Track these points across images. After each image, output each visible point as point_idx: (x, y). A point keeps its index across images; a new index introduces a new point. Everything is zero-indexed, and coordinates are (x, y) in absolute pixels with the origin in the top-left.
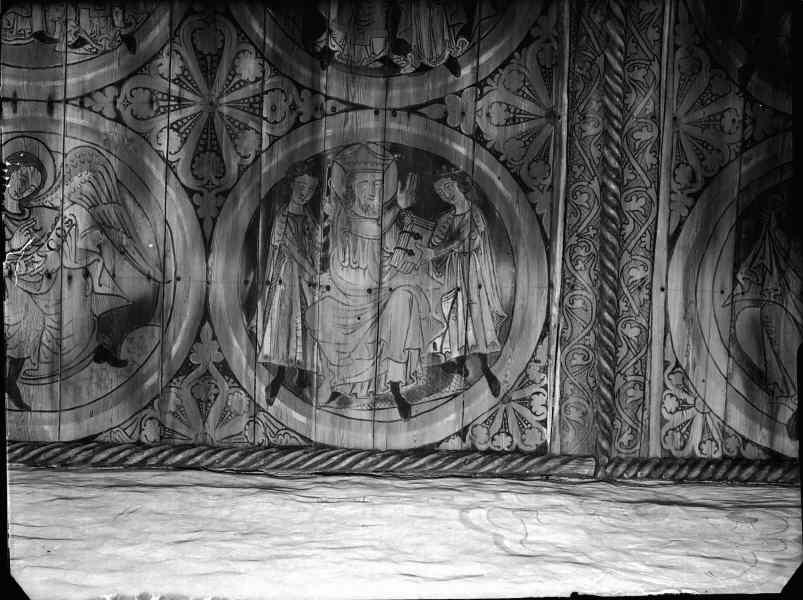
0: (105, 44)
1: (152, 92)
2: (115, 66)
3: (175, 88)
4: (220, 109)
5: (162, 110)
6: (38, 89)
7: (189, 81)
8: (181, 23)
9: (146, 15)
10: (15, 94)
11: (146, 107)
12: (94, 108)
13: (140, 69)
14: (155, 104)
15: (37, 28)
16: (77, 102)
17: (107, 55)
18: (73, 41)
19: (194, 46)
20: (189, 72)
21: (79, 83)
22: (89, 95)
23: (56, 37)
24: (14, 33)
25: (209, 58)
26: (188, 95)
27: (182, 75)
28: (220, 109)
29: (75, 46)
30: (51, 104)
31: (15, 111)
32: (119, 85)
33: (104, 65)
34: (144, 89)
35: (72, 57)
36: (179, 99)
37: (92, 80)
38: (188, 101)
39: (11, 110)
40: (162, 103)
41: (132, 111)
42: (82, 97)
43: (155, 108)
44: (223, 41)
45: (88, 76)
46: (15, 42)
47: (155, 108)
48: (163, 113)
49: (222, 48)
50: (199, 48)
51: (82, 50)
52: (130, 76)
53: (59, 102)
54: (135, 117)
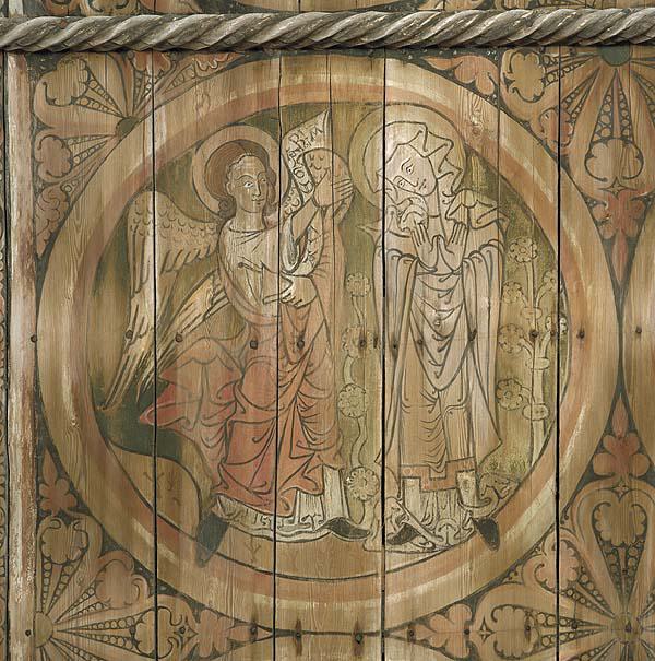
0: (448, 534)
1: (528, 613)
2: (465, 568)
3: (565, 603)
4: (644, 636)
5: (546, 642)
6: (340, 612)
7: (599, 602)
8: (576, 493)
9: (514, 485)
10: (299, 624)
11: (520, 637)
12: (431, 643)
13: (506, 575)
14: (533, 632)
15: (335, 509)
16: (403, 633)
17: (451, 551)
18: (396, 533)
19: (598, 534)
20: (590, 576)
21: (405, 601)
22: (424, 621)
23: (365, 526)
24: (296, 523)
25: (622, 552)
26: (590, 616)
27: (578, 581)
28: (644, 636)
29: (399, 540)
30: (359, 637)
31: (299, 651)
32: (472, 601)
33: (443, 571)
34: (515, 607)
35: (395, 560)
36: (575, 623)
37: (428, 595)
38: (591, 624)
39: (294, 651)
40: (544, 631)
41: (495, 643)
42: (410, 625)
43: (534, 638)
44: (645, 524)
45: (421, 589)
46: (297, 538)
47: (534, 638)
48: (547, 647)
49: (644, 536)
50: (605, 536)
51: (409, 547)
52: (490, 587)
53: (372, 634)
54: (502, 655)
